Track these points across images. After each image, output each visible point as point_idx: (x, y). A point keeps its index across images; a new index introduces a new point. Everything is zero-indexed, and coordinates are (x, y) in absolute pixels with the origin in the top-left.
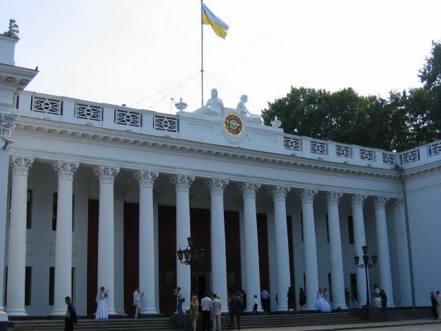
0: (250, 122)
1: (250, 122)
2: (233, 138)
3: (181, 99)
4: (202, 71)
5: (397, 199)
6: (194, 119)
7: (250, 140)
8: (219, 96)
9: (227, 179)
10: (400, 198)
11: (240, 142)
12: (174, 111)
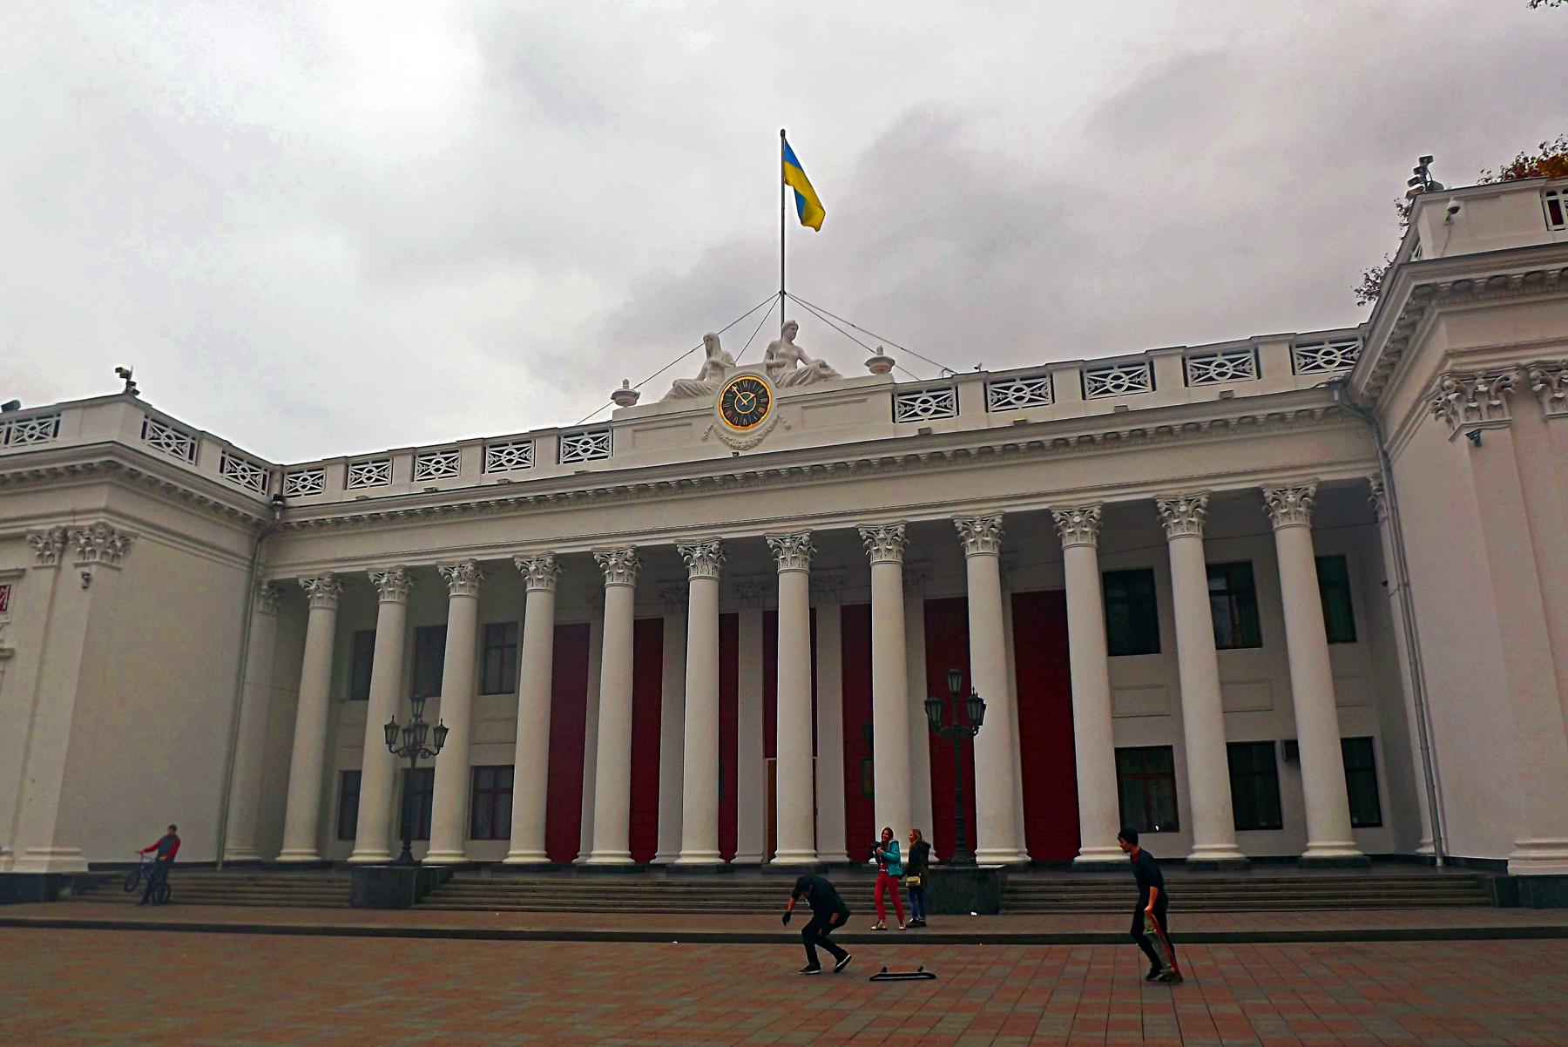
0: (791, 383)
1: (791, 383)
2: (744, 435)
3: (626, 383)
4: (783, 293)
5: (1366, 481)
6: (656, 420)
7: (788, 428)
8: (724, 346)
9: (804, 529)
10: (1368, 474)
11: (760, 441)
12: (606, 412)
